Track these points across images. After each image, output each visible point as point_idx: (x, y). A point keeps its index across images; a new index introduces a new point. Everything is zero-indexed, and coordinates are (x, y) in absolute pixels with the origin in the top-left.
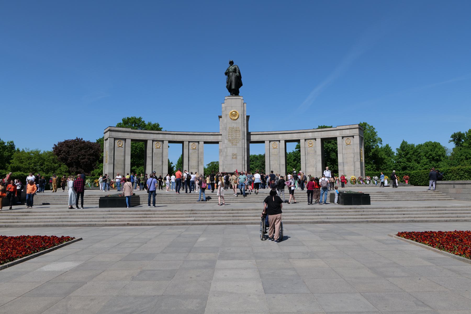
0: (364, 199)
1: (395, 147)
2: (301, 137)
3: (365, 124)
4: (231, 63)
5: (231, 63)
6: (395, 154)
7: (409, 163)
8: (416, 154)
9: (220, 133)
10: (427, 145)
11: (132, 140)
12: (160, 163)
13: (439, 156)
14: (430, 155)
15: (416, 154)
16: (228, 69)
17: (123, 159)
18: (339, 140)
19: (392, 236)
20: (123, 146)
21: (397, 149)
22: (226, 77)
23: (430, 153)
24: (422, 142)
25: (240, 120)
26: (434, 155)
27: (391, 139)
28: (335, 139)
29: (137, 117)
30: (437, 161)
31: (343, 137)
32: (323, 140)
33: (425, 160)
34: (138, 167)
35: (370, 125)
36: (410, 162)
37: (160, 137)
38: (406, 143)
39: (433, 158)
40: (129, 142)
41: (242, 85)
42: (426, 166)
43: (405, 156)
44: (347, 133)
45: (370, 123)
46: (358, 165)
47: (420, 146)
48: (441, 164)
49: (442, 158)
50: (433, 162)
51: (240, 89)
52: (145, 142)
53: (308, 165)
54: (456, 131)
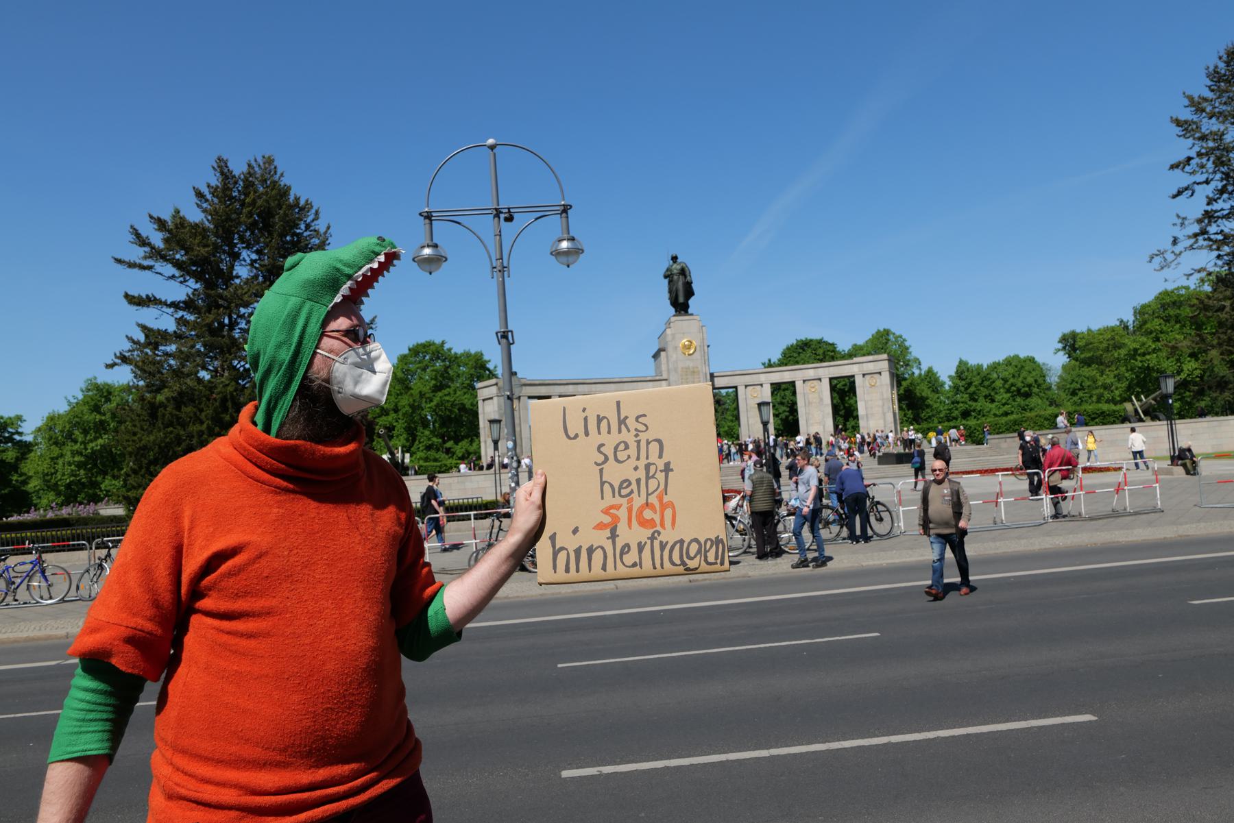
1: (946, 372)
3: (887, 332)
4: (674, 259)
5: (674, 259)
6: (947, 387)
7: (974, 404)
8: (986, 383)
9: (665, 376)
10: (1009, 362)
13: (1030, 386)
14: (1012, 385)
15: (986, 383)
21: (950, 377)
22: (666, 281)
23: (1012, 381)
24: (1000, 357)
25: (697, 355)
26: (1019, 385)
27: (939, 358)
29: (438, 341)
30: (1027, 395)
31: (864, 375)
33: (1003, 396)
34: (456, 443)
35: (898, 334)
36: (976, 400)
38: (966, 363)
39: (1019, 390)
41: (693, 294)
42: (1006, 408)
43: (966, 389)
44: (870, 367)
45: (896, 330)
47: (995, 367)
48: (1034, 401)
49: (1035, 390)
50: (1018, 399)
51: (691, 302)
54: (1067, 330)
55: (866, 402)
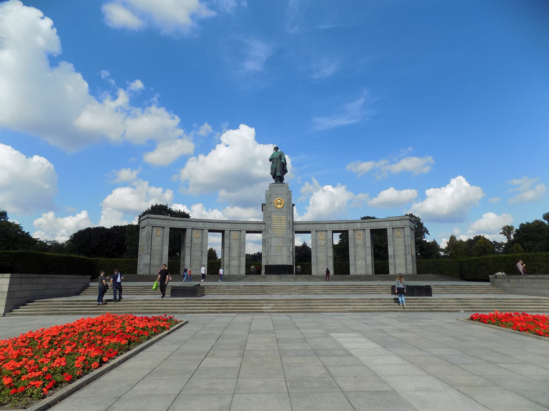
0: (427, 291)
2: (349, 228)
11: (171, 229)
12: (199, 254)
16: (272, 155)
17: (161, 249)
18: (389, 232)
19: (459, 320)
20: (161, 235)
28: (386, 230)
32: (372, 231)
37: (200, 225)
40: (167, 231)
44: (398, 224)
46: (409, 258)
52: (184, 230)
53: (357, 257)
55: (394, 247)
